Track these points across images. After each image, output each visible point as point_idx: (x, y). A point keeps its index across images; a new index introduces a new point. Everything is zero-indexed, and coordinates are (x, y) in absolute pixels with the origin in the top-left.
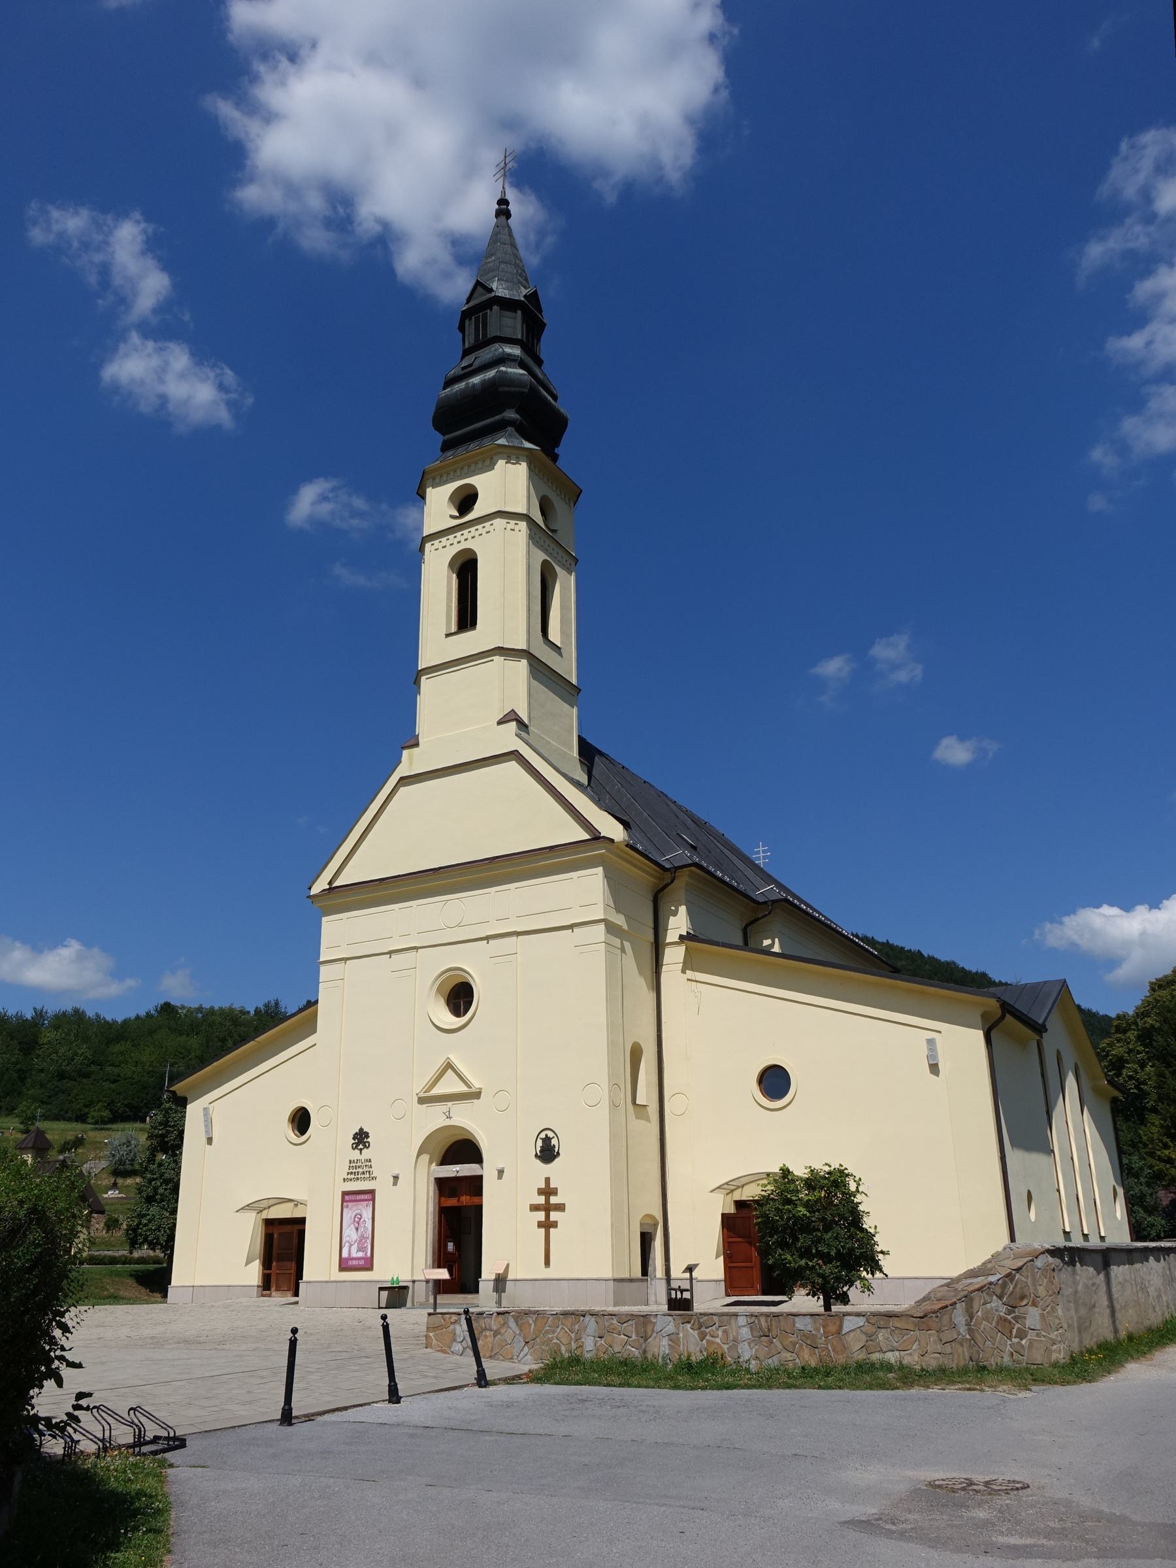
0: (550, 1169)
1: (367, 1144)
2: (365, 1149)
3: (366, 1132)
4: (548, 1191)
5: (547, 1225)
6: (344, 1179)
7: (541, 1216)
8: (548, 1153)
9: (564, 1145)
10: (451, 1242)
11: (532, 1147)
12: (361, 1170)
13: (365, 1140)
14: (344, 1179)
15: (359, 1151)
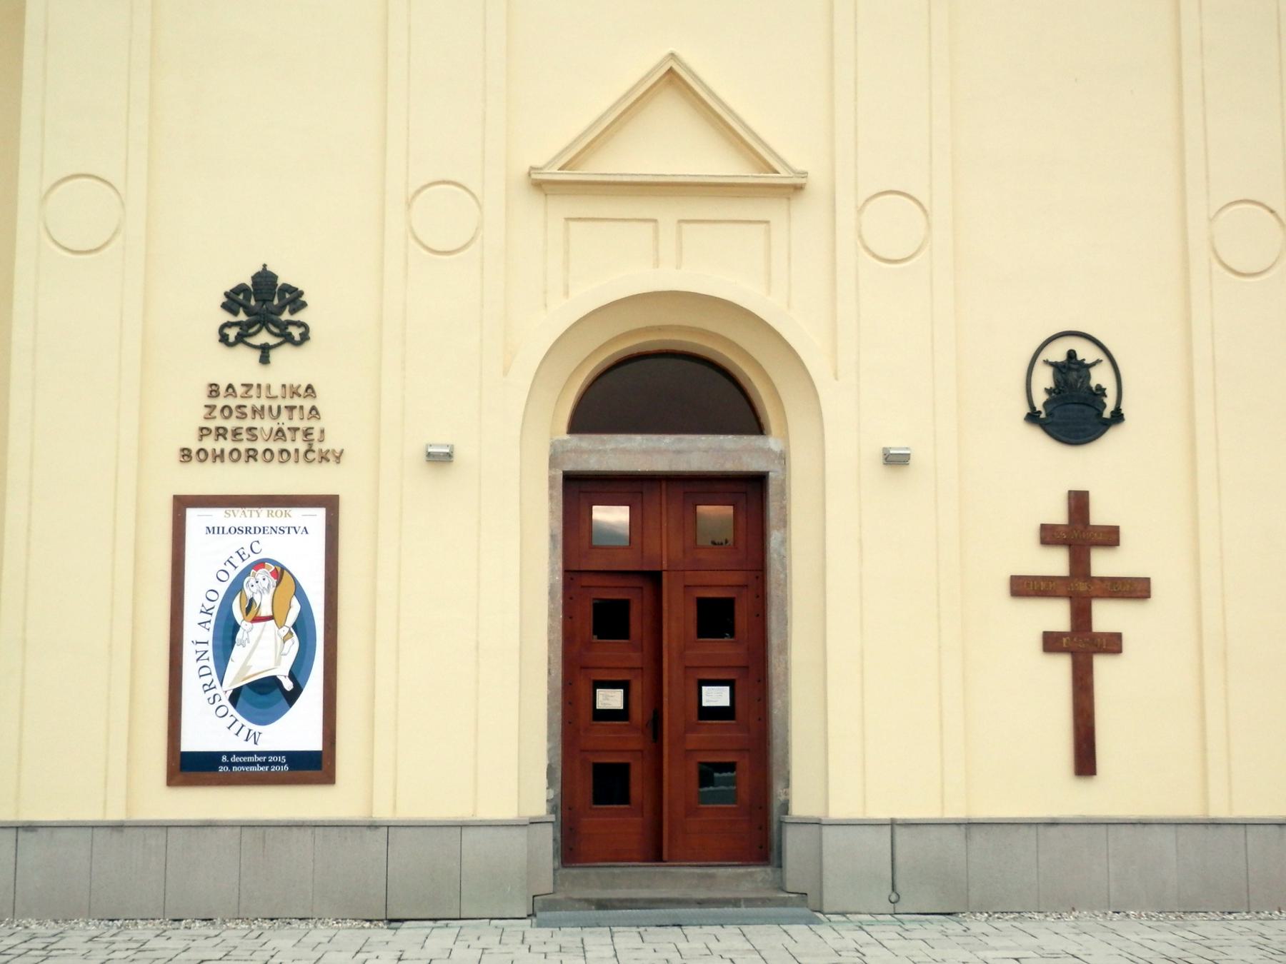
1: (296, 332)
2: (287, 349)
3: (287, 288)
6: (186, 454)
7: (1057, 616)
12: (266, 424)
13: (286, 316)
14: (186, 454)
15: (256, 355)
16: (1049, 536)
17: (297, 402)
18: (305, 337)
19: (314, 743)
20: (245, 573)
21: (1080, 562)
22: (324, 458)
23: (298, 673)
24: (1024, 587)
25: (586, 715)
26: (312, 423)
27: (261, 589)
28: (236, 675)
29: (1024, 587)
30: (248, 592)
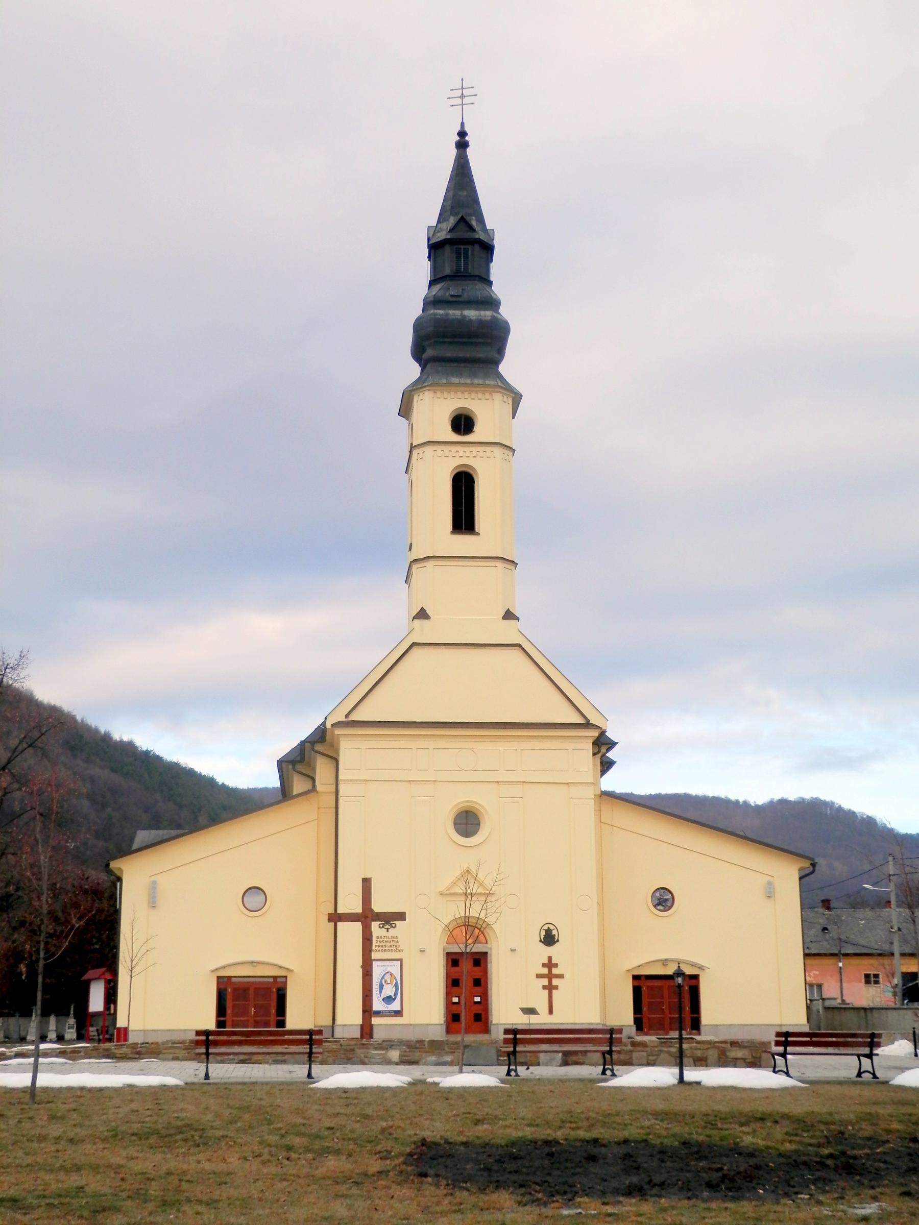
0: (553, 951)
1: (394, 925)
4: (550, 965)
5: (550, 988)
8: (549, 939)
9: (563, 934)
10: (456, 997)
11: (536, 935)
12: (388, 944)
16: (544, 965)
18: (395, 926)
19: (399, 1009)
20: (385, 974)
21: (550, 971)
22: (399, 951)
23: (395, 995)
24: (539, 976)
25: (450, 1004)
27: (388, 977)
28: (383, 995)
29: (539, 976)
30: (385, 978)
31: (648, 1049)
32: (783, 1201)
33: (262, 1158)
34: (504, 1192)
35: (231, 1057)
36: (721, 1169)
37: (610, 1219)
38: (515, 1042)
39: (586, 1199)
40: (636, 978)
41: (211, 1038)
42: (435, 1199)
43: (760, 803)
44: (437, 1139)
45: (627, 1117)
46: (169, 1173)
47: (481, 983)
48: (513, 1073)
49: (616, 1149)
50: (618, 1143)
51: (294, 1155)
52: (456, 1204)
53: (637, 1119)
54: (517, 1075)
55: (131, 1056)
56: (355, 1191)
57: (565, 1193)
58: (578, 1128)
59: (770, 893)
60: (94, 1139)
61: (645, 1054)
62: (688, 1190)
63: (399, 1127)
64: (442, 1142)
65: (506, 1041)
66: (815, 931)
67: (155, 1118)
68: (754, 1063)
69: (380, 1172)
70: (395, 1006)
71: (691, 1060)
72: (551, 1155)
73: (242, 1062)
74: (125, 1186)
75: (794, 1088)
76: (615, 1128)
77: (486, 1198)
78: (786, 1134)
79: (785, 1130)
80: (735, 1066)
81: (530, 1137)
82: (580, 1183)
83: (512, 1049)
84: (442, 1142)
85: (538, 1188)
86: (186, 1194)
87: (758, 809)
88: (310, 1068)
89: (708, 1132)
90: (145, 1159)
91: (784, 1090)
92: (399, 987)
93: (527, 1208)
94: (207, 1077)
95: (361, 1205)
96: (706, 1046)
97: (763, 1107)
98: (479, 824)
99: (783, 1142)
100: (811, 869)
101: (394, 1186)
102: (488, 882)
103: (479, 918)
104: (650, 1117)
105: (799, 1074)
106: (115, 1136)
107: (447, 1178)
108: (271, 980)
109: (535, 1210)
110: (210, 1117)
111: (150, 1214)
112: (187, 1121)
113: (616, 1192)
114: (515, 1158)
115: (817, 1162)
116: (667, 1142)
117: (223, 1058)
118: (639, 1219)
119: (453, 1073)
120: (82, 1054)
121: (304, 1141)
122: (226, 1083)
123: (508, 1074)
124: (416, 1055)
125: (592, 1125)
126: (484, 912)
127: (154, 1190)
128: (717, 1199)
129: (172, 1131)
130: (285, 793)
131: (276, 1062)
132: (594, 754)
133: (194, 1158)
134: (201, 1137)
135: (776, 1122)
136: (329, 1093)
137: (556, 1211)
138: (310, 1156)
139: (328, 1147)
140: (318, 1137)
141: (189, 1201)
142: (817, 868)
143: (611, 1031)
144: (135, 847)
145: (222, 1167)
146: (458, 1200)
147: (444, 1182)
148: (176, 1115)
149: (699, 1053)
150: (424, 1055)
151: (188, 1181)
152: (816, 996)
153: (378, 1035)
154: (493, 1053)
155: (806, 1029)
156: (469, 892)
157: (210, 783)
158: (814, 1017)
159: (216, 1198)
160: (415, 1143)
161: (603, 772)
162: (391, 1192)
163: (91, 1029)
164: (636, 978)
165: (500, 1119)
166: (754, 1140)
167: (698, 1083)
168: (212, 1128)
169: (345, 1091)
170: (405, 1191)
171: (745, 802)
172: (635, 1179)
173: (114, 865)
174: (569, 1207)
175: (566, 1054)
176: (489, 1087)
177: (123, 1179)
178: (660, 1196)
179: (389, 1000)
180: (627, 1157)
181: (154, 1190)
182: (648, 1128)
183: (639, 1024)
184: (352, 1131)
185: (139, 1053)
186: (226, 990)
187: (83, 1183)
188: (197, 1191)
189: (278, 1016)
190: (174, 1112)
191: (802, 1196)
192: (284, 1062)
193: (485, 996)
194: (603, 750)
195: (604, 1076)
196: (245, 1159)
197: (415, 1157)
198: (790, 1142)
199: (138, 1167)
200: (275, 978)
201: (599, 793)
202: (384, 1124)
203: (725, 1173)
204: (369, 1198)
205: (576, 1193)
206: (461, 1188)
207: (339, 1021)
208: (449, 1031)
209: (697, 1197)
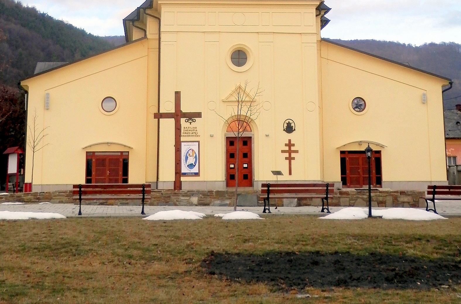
1: (194, 120)
4: (290, 144)
5: (290, 159)
7: (287, 155)
8: (289, 129)
10: (232, 164)
11: (281, 127)
12: (191, 132)
16: (286, 145)
17: (194, 129)
18: (195, 121)
20: (189, 151)
21: (290, 148)
24: (283, 151)
25: (229, 168)
26: (196, 132)
27: (190, 152)
29: (283, 151)
31: (350, 196)
32: (432, 289)
33: (113, 263)
34: (262, 284)
35: (95, 201)
36: (394, 270)
37: (326, 300)
38: (269, 192)
39: (312, 288)
40: (342, 152)
41: (82, 189)
42: (220, 288)
43: (418, 45)
44: (221, 251)
45: (337, 238)
46: (57, 272)
47: (247, 156)
48: (267, 211)
49: (330, 258)
50: (332, 254)
51: (133, 261)
52: (232, 291)
53: (343, 239)
54: (270, 212)
55: (33, 200)
56: (170, 283)
57: (299, 284)
58: (307, 245)
59: (424, 101)
60: (11, 251)
61: (348, 199)
62: (374, 283)
63: (197, 244)
64: (224, 253)
65: (263, 191)
66: (452, 124)
67: (48, 238)
68: (415, 205)
69: (186, 272)
70: (195, 170)
71: (376, 203)
72: (290, 261)
73: (102, 204)
74: (30, 280)
75: (439, 220)
76: (329, 245)
77: (251, 287)
78: (434, 248)
79: (433, 246)
80: (403, 207)
81: (277, 250)
82: (308, 278)
83: (266, 196)
84: (224, 253)
85: (282, 281)
86: (67, 285)
87: (417, 50)
88: (143, 208)
89: (386, 247)
90: (42, 264)
91: (433, 221)
92: (197, 158)
93: (275, 294)
94: (80, 213)
95: (174, 292)
96: (385, 195)
97: (420, 232)
98: (246, 58)
99: (432, 253)
100: (450, 86)
101: (194, 280)
102: (252, 94)
103: (246, 116)
104: (351, 238)
105: (442, 212)
106: (24, 249)
107: (226, 275)
108: (119, 154)
109: (281, 295)
110: (82, 238)
111: (45, 297)
112: (67, 241)
113: (330, 284)
114: (269, 263)
115: (453, 266)
116: (362, 253)
117: (90, 202)
118: (344, 300)
119: (230, 211)
120: (3, 199)
121: (140, 252)
122: (91, 217)
123: (264, 211)
124: (208, 200)
125: (316, 243)
126: (249, 112)
127: (47, 282)
128: (392, 288)
129: (59, 247)
130: (128, 40)
131: (123, 204)
132: (317, 16)
133: (72, 263)
134: (76, 250)
135: (428, 241)
136: (155, 223)
137: (294, 296)
138: (143, 262)
139: (154, 256)
140: (148, 250)
141: (69, 289)
142: (453, 85)
143: (327, 185)
144: (36, 72)
145: (89, 268)
146: (233, 289)
147: (225, 278)
148: (61, 237)
149: (381, 199)
150: (213, 200)
151: (68, 277)
152: (452, 164)
153: (185, 188)
154: (255, 199)
155: (447, 184)
156: (240, 100)
157: (82, 33)
158: (451, 177)
159: (85, 287)
160: (207, 254)
161: (322, 27)
162: (193, 284)
163: (9, 184)
164: (342, 152)
165: (259, 239)
166: (415, 252)
167: (381, 217)
168: (83, 244)
169: (165, 222)
170: (201, 283)
171: (409, 45)
172: (342, 276)
173: (23, 83)
174: (302, 293)
175: (299, 199)
176: (252, 219)
177: (28, 276)
178: (357, 286)
179: (191, 166)
180: (337, 262)
181: (47, 282)
182: (350, 244)
183: (344, 181)
184: (169, 246)
185: (38, 199)
186: (91, 160)
187: (5, 278)
188: (74, 283)
189: (123, 176)
190: (60, 235)
191: (444, 286)
192: (127, 204)
193: (250, 163)
194: (322, 13)
195: (323, 213)
196: (104, 263)
197: (207, 262)
198: (437, 253)
199: (38, 268)
200: (122, 152)
201: (320, 39)
202: (189, 242)
203: (397, 272)
204: (179, 287)
205: (306, 284)
206: (236, 282)
207: (160, 179)
208: (228, 185)
209: (379, 287)
